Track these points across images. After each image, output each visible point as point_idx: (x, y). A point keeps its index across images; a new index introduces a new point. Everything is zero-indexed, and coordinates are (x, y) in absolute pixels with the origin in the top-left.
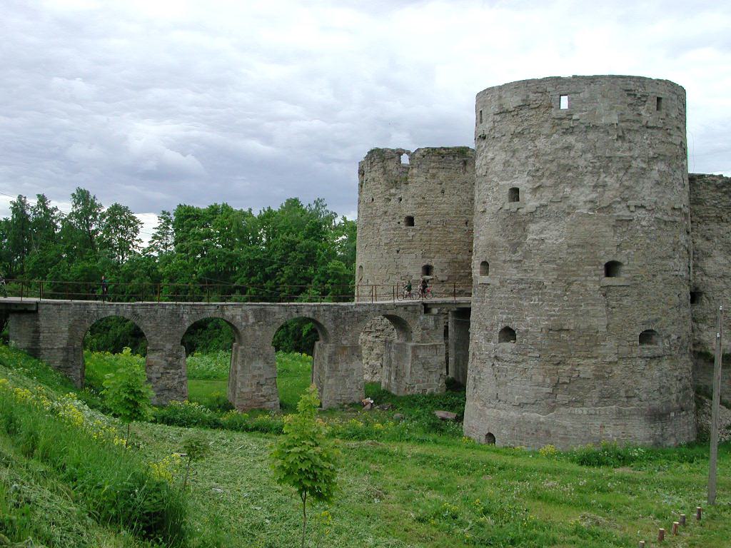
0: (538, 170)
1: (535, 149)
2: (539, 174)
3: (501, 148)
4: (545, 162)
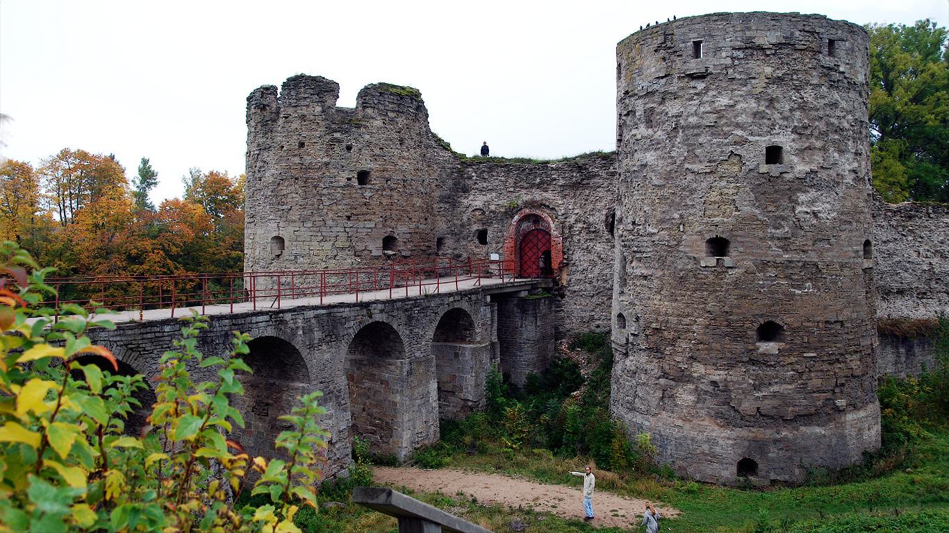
0: (806, 128)
1: (800, 100)
2: (808, 132)
3: (750, 94)
4: (814, 119)
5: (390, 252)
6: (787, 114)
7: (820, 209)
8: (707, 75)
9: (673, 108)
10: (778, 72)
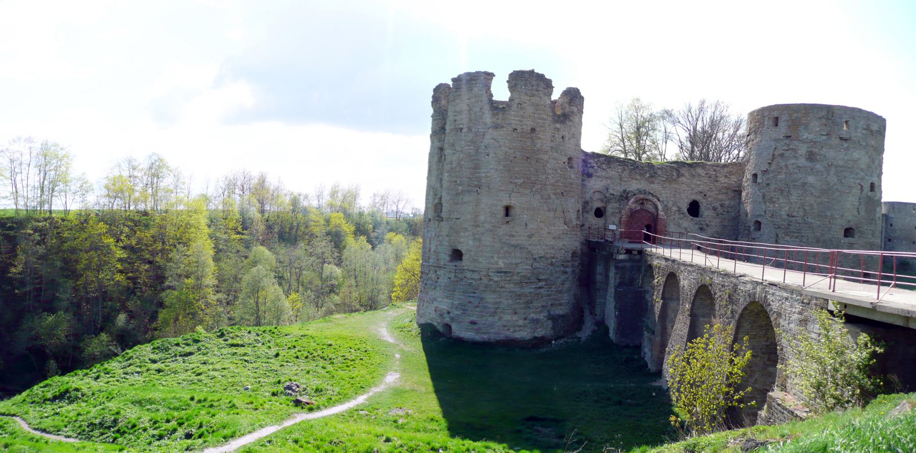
9: (831, 154)
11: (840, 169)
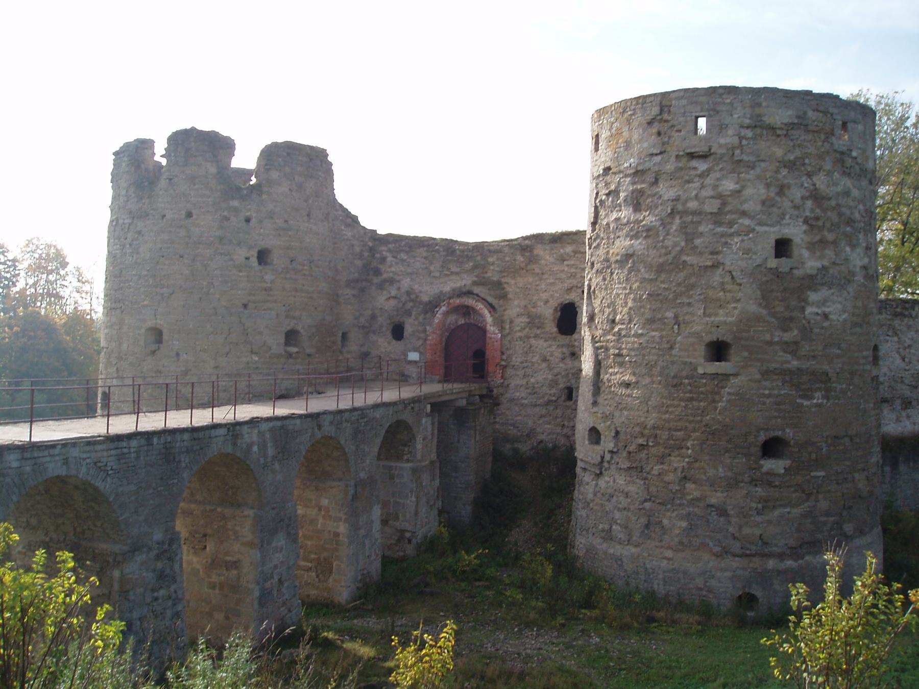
2: (820, 223)
3: (758, 177)
5: (293, 350)
6: (798, 201)
7: (831, 309)
8: (711, 154)
10: (789, 155)
11: (689, 219)
